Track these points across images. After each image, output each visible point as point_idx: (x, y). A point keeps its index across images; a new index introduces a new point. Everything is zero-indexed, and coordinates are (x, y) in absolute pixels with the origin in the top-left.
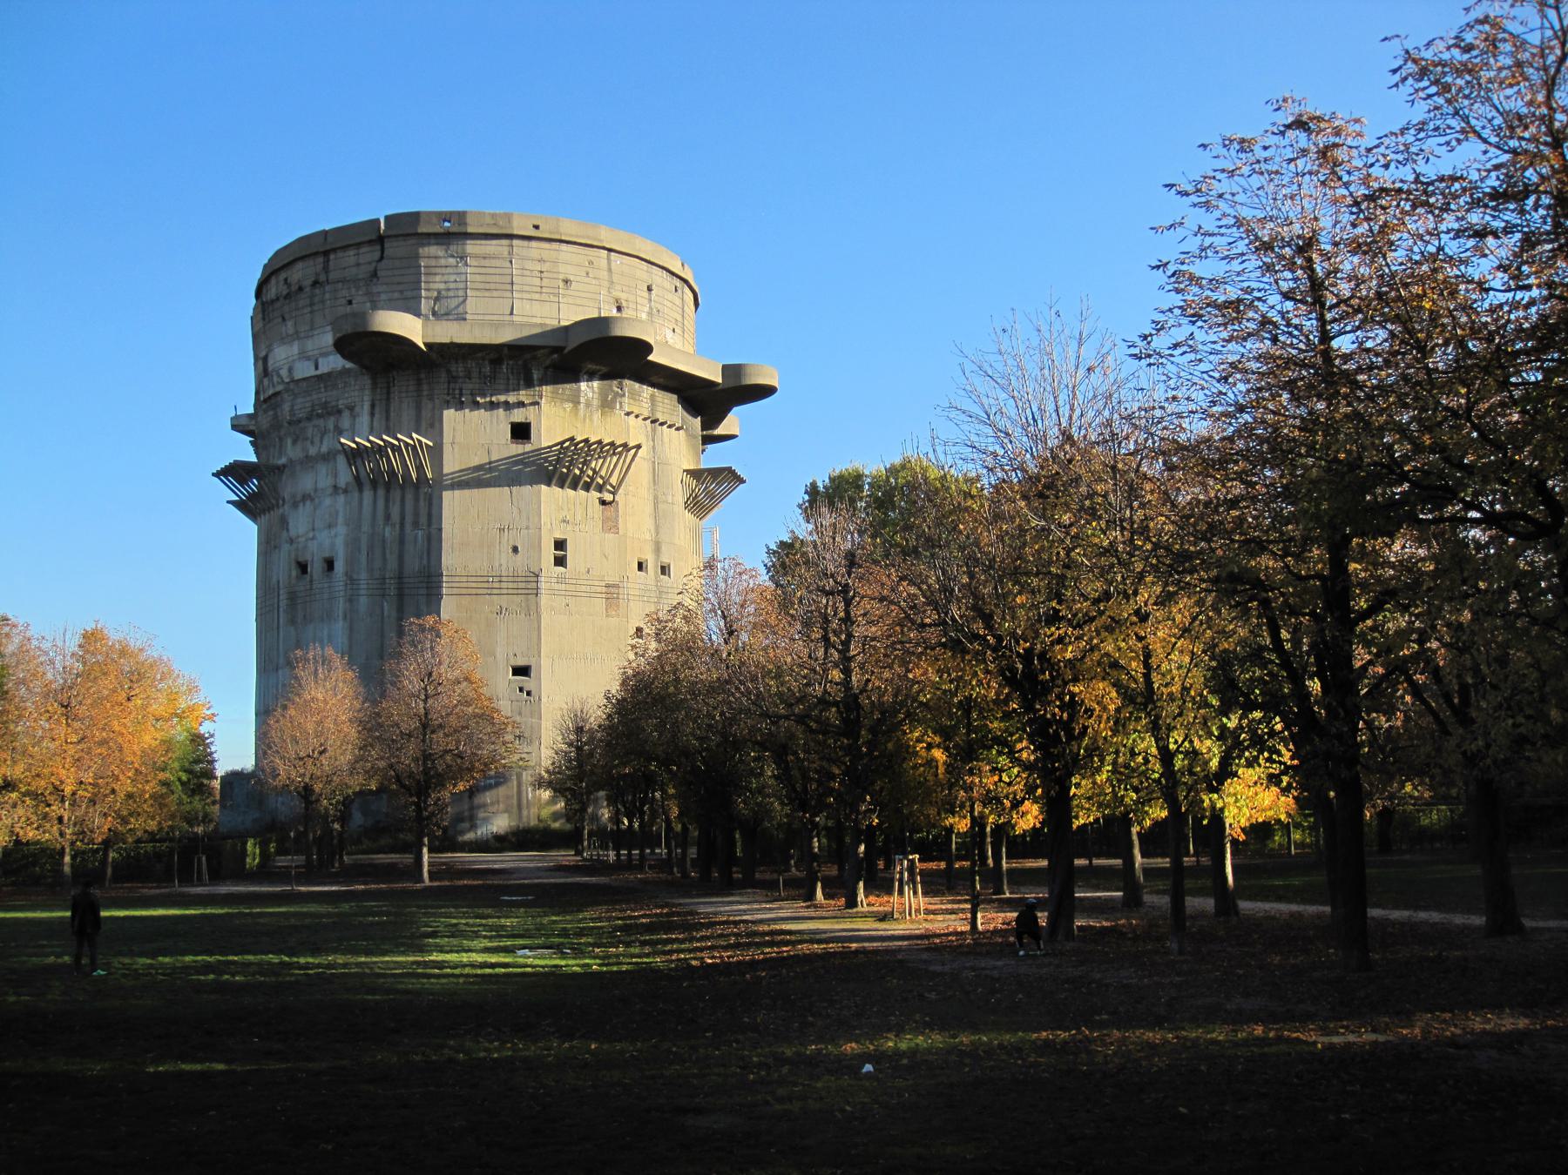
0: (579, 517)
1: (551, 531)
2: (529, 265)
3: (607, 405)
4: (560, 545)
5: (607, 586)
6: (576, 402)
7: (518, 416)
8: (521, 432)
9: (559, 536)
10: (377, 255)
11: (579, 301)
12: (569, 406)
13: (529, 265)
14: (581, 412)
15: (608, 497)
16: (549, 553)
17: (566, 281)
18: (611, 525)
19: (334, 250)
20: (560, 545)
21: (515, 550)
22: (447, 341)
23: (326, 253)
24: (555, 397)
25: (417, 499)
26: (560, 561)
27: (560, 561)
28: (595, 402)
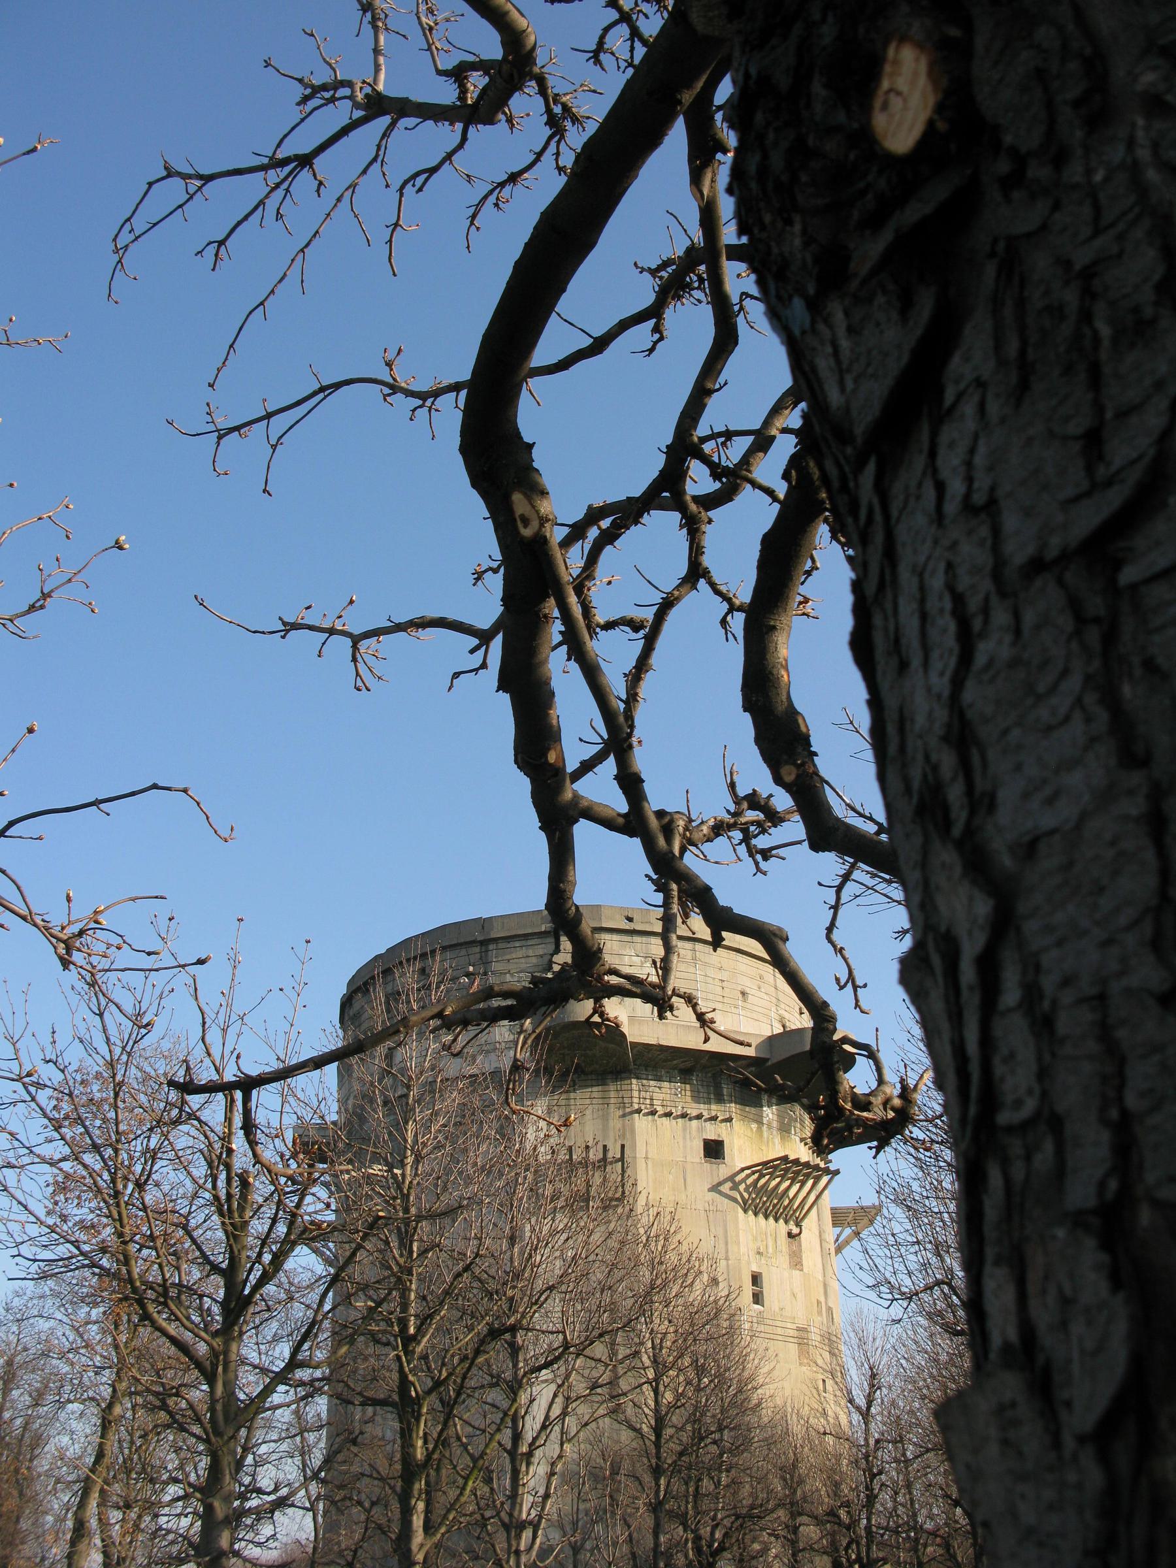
0: (770, 1250)
1: (749, 1263)
2: (711, 972)
3: (784, 1129)
4: (756, 1279)
5: (799, 1329)
6: (760, 1122)
7: (712, 1132)
8: (714, 1150)
9: (755, 1269)
10: (552, 947)
11: (755, 1016)
12: (754, 1126)
13: (711, 972)
14: (765, 1134)
15: (795, 1230)
16: (748, 1289)
17: (743, 994)
18: (796, 1261)
19: (495, 940)
20: (756, 1279)
22: (653, 1042)
23: (484, 943)
24: (744, 1117)
26: (757, 1298)
27: (757, 1298)
28: (775, 1124)
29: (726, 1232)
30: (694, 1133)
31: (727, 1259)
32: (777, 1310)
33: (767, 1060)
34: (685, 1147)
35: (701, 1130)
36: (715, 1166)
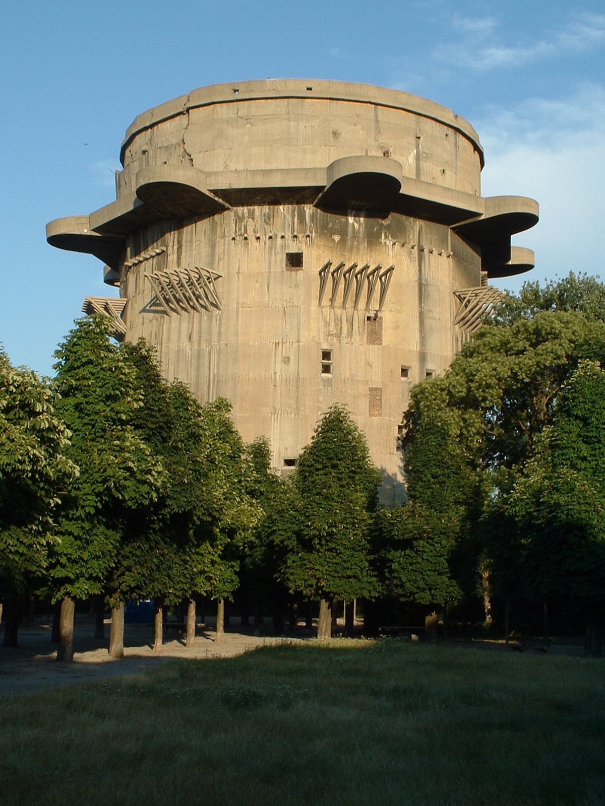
1: (319, 344)
4: (326, 355)
5: (371, 389)
8: (295, 260)
9: (325, 347)
18: (375, 337)
20: (326, 355)
21: (286, 360)
25: (210, 319)
26: (326, 369)
27: (326, 369)
29: (299, 321)
30: (278, 250)
31: (298, 341)
32: (348, 376)
33: (325, 186)
34: (270, 260)
35: (283, 247)
36: (294, 273)
